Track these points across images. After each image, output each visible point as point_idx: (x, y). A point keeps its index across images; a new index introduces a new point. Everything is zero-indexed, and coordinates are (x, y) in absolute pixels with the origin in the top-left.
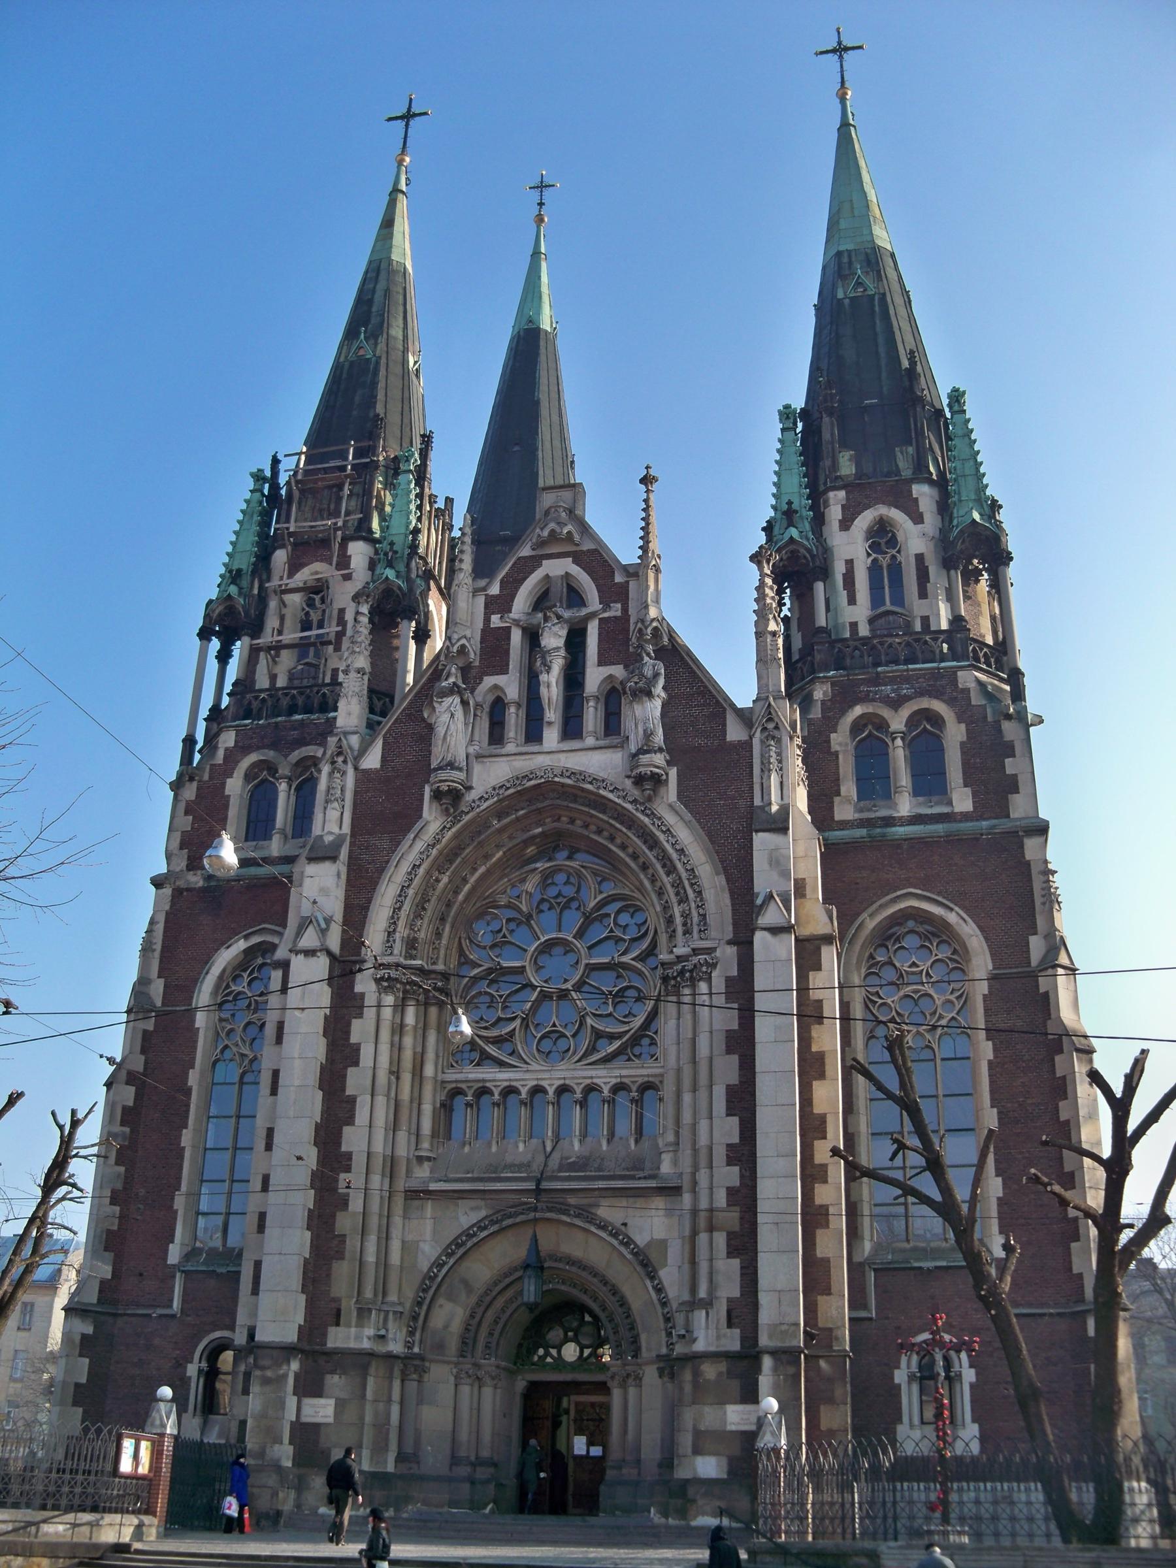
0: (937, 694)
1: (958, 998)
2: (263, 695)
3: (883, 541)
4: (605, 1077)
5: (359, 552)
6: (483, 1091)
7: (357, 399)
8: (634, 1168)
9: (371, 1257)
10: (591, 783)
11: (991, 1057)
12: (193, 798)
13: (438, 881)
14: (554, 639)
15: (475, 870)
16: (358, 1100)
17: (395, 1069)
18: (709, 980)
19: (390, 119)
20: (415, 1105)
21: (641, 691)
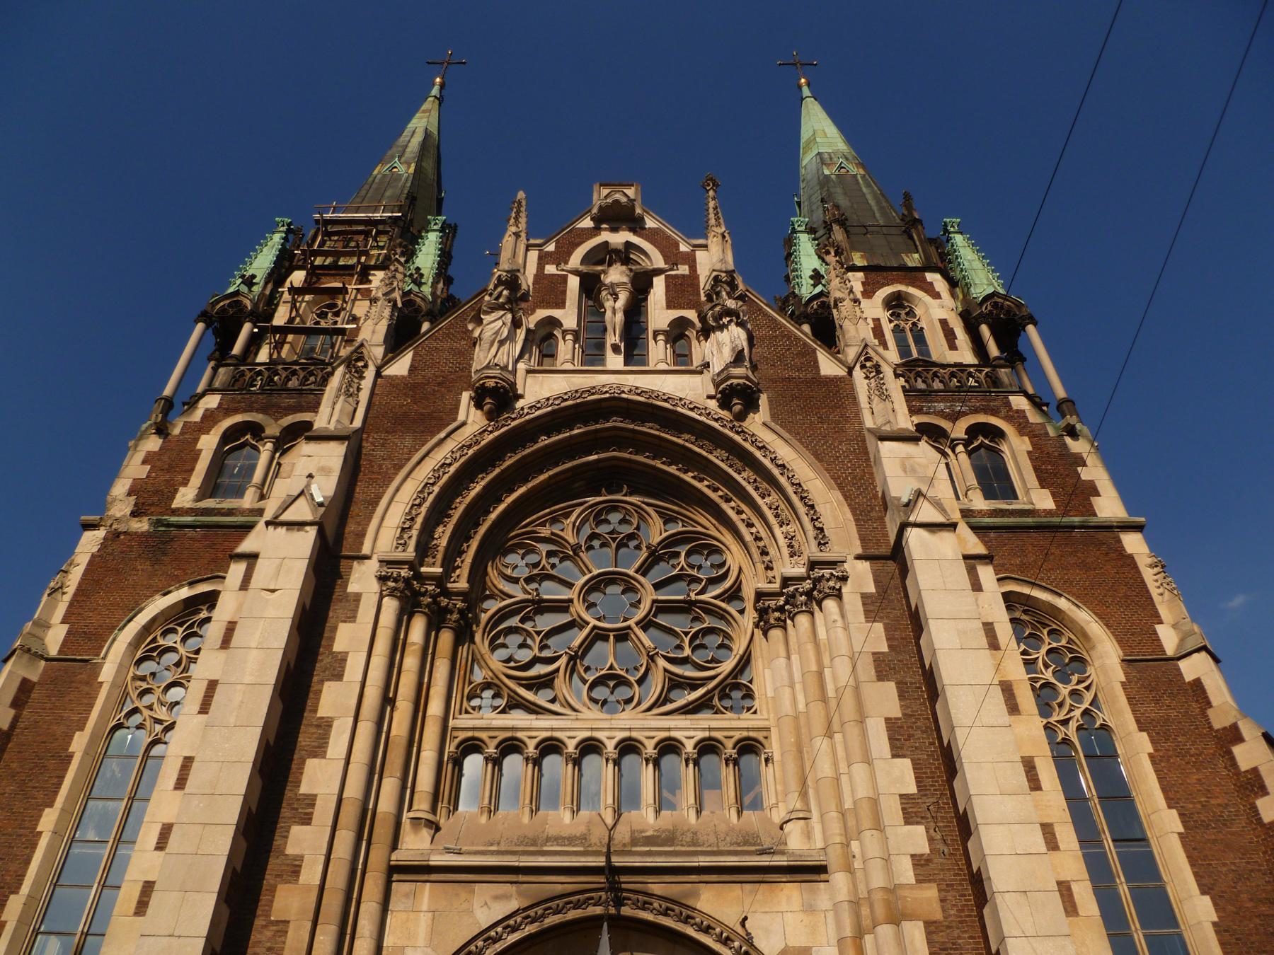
0: (995, 413)
1: (1087, 688)
2: (259, 368)
3: (903, 312)
4: (689, 730)
6: (511, 746)
7: (388, 193)
8: (746, 843)
10: (665, 401)
11: (1151, 750)
16: (335, 724)
18: (838, 595)
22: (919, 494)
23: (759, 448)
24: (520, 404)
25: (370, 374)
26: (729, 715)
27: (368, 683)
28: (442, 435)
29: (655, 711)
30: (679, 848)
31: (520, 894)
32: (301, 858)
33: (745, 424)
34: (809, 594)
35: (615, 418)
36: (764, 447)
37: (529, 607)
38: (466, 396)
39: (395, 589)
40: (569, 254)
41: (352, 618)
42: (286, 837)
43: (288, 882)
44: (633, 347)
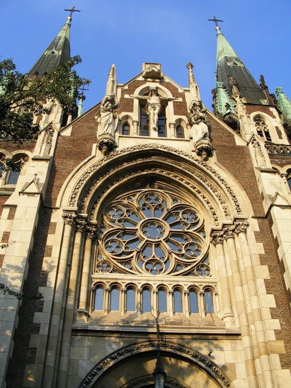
3: (261, 123)
4: (186, 282)
8: (210, 325)
9: (51, 362)
10: (175, 151)
15: (113, 185)
17: (69, 263)
18: (246, 232)
20: (79, 285)
22: (278, 194)
23: (213, 173)
24: (117, 149)
25: (55, 134)
26: (201, 277)
27: (61, 258)
28: (86, 160)
29: (172, 274)
30: (184, 326)
31: (124, 342)
32: (40, 324)
33: (207, 162)
34: (233, 231)
35: (154, 157)
36: (215, 172)
37: (119, 231)
38: (94, 146)
39: (70, 221)
40: (134, 91)
41: (54, 232)
42: (33, 316)
43: (35, 334)
44: (161, 130)
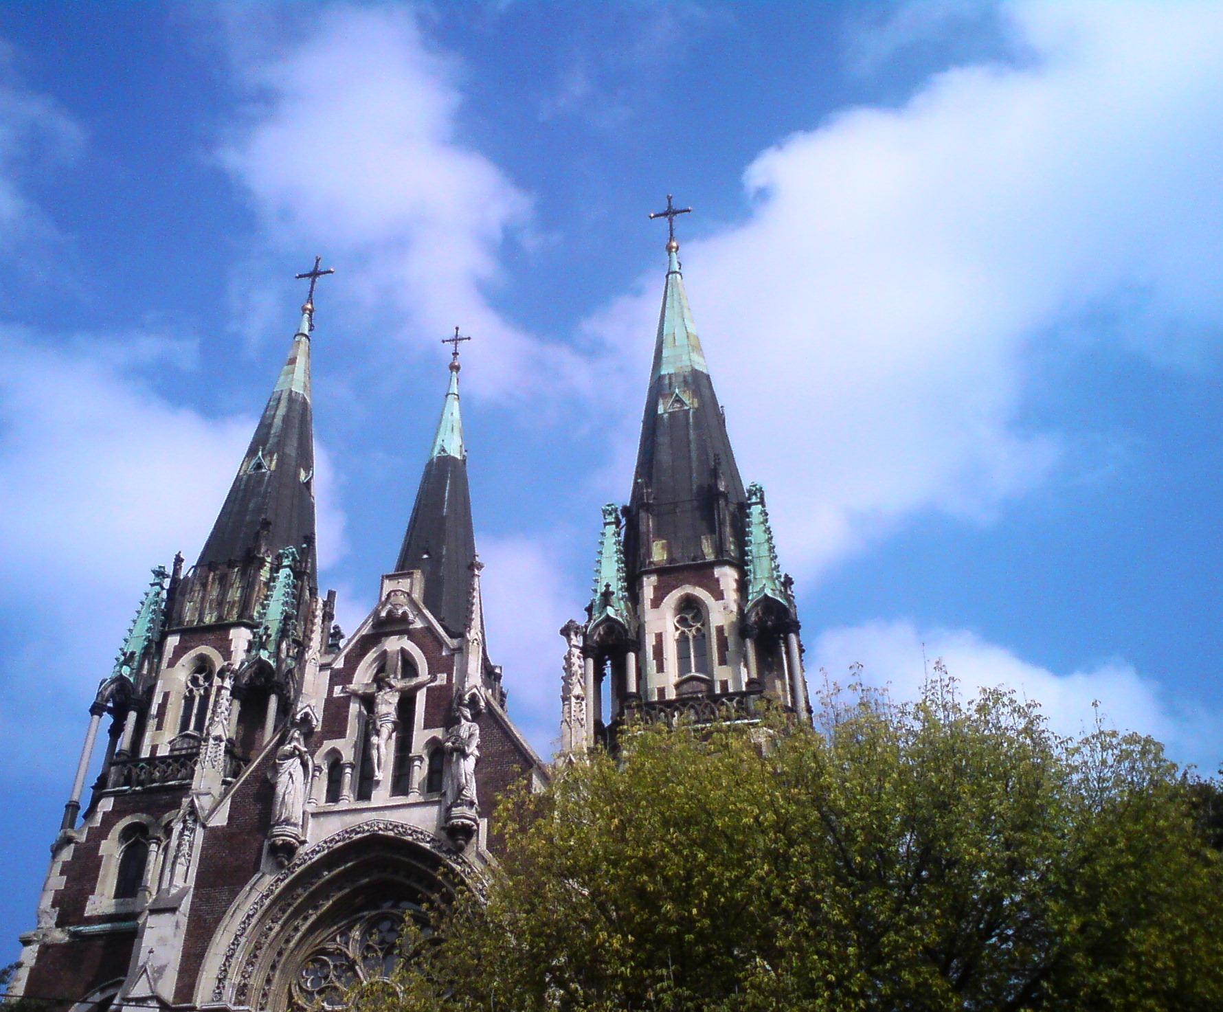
3: (689, 617)
5: (240, 638)
7: (251, 506)
10: (411, 835)
12: (70, 859)
13: (271, 929)
14: (388, 705)
19: (300, 276)
21: (457, 750)
